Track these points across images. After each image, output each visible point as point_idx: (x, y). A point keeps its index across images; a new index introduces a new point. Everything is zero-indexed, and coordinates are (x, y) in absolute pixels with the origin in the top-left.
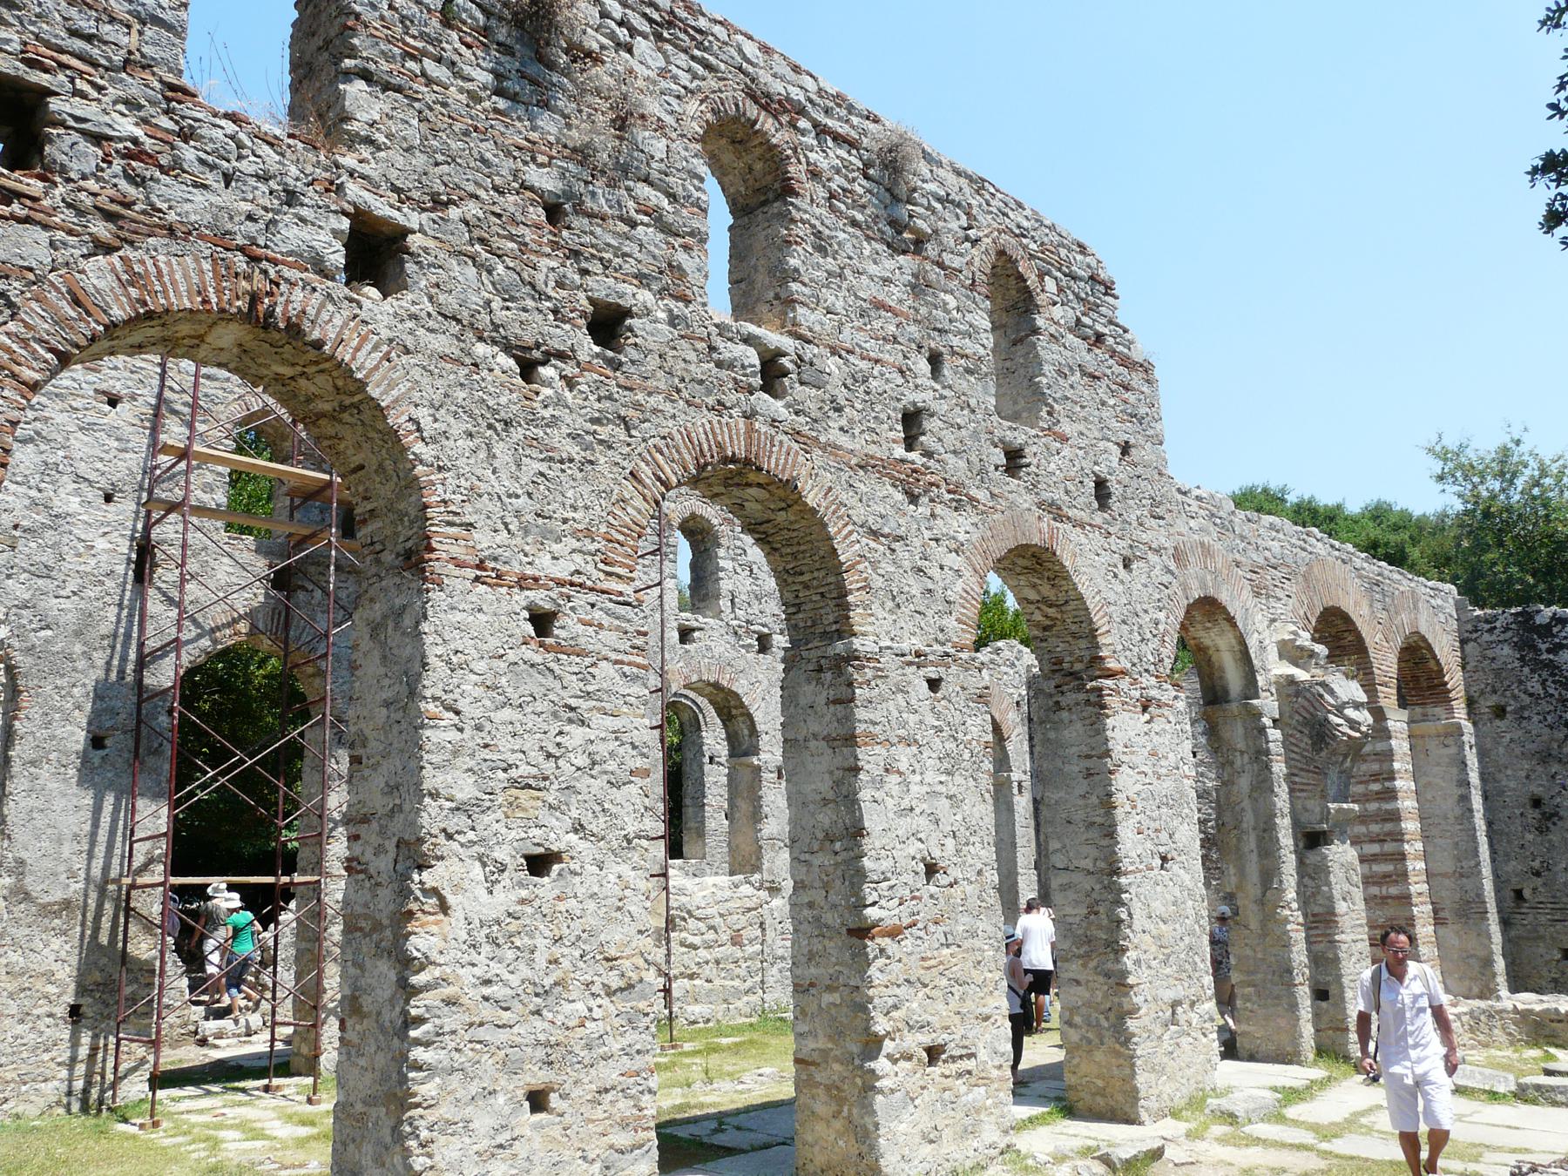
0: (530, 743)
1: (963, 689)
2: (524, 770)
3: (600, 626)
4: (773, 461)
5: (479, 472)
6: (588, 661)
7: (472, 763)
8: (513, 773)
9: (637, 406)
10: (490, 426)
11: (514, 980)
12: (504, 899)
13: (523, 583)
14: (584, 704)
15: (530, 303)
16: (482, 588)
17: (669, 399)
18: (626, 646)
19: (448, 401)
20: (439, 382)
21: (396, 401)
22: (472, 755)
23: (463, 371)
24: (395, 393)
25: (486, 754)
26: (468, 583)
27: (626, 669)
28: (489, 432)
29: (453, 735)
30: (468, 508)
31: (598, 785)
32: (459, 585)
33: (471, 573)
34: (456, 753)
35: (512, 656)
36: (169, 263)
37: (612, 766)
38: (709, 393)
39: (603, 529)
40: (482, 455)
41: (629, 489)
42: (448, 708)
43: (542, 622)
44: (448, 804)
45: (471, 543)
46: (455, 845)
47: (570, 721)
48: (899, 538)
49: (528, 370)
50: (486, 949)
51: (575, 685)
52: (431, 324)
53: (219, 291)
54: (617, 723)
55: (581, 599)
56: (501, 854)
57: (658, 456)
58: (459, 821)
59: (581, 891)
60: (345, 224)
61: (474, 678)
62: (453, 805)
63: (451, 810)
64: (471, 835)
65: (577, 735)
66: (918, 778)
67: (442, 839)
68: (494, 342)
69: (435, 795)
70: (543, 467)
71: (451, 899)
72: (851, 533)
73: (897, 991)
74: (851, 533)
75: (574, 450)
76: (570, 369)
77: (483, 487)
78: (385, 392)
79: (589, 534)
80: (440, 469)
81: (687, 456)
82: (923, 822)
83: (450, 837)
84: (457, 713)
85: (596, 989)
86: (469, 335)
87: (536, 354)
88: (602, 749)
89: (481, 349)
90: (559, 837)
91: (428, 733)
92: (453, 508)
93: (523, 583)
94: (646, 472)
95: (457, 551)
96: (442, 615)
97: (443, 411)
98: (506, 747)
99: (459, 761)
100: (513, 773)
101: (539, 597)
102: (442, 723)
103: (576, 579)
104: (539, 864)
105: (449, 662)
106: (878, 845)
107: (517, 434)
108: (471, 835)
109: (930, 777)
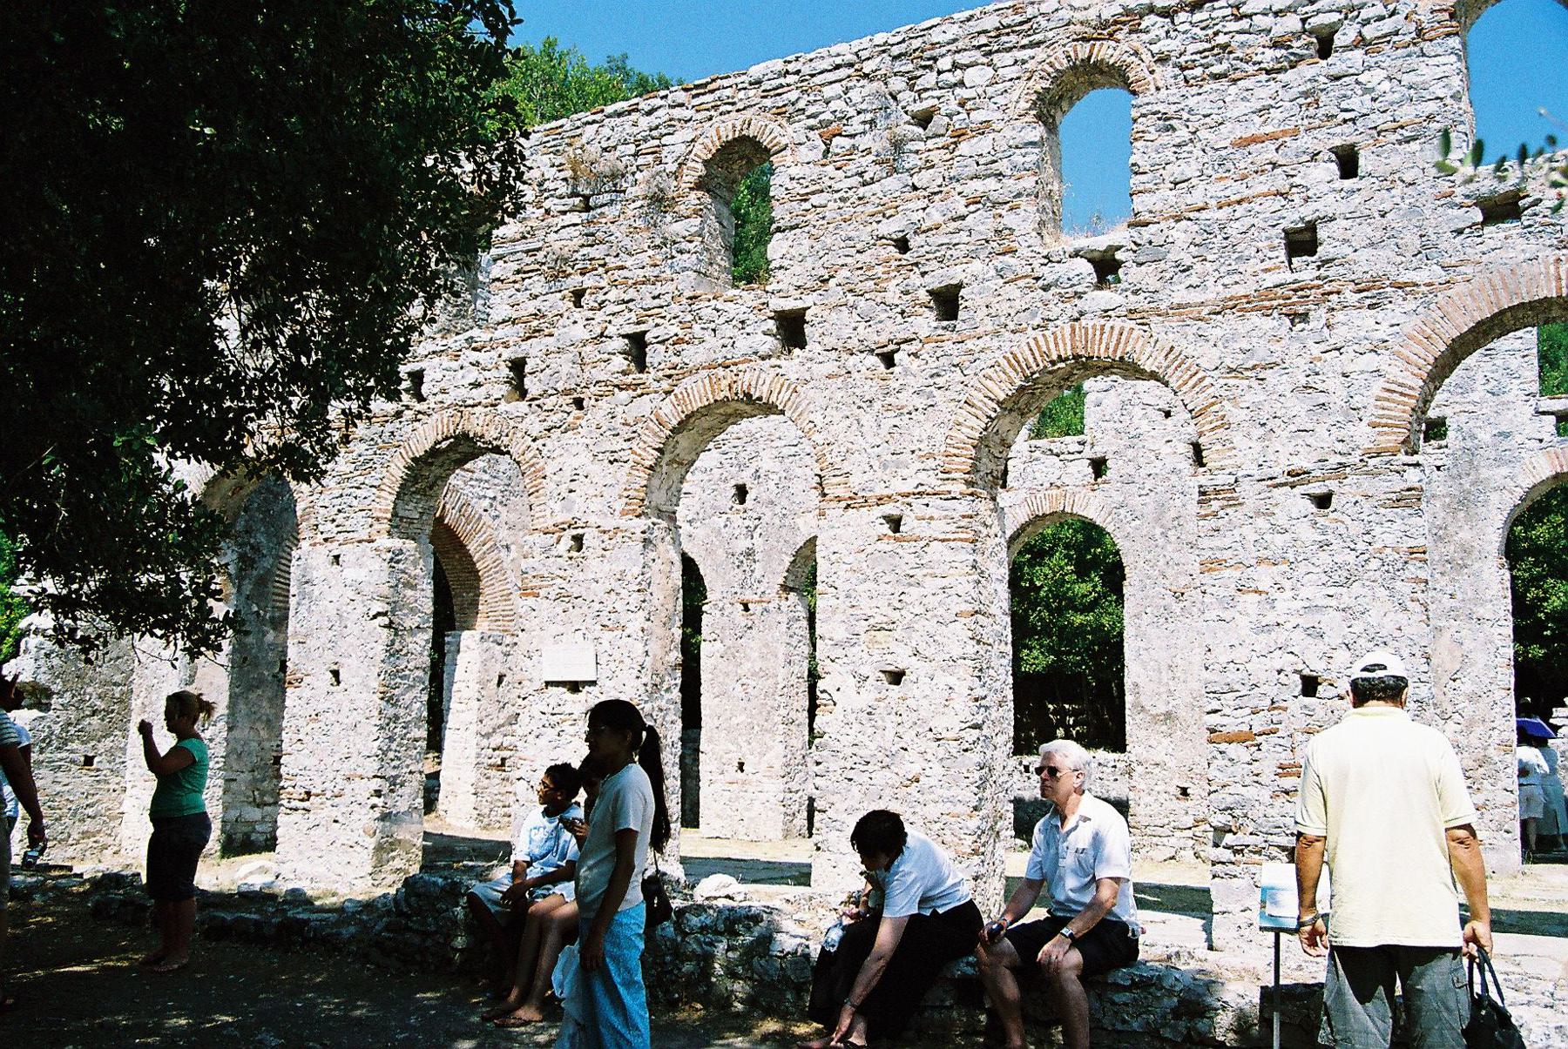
0: (882, 602)
1: (1367, 497)
2: (879, 619)
3: (931, 518)
4: (1103, 347)
6: (923, 543)
8: (872, 621)
9: (970, 352)
11: (873, 746)
12: (868, 697)
13: (880, 500)
14: (919, 573)
15: (883, 316)
17: (997, 334)
18: (953, 528)
25: (851, 611)
27: (952, 544)
29: (833, 602)
31: (931, 626)
33: (843, 504)
34: (834, 612)
35: (869, 550)
37: (941, 611)
38: (1034, 315)
39: (943, 449)
41: (962, 415)
43: (895, 523)
47: (910, 585)
48: (1272, 365)
49: (888, 360)
50: (856, 726)
51: (912, 560)
52: (821, 359)
53: (713, 392)
54: (945, 582)
55: (917, 504)
56: (864, 671)
57: (988, 383)
58: (838, 652)
59: (917, 693)
60: (771, 325)
65: (915, 592)
66: (1288, 594)
70: (897, 421)
72: (1202, 380)
73: (1243, 790)
74: (1202, 380)
75: (920, 402)
76: (913, 347)
77: (854, 447)
79: (930, 456)
81: (1013, 374)
82: (1298, 635)
85: (928, 756)
86: (844, 356)
87: (892, 347)
88: (932, 601)
89: (852, 361)
90: (901, 661)
93: (880, 500)
94: (977, 398)
98: (866, 607)
100: (872, 621)
101: (890, 509)
103: (921, 489)
104: (896, 677)
106: (1223, 659)
107: (877, 405)
109: (1304, 592)
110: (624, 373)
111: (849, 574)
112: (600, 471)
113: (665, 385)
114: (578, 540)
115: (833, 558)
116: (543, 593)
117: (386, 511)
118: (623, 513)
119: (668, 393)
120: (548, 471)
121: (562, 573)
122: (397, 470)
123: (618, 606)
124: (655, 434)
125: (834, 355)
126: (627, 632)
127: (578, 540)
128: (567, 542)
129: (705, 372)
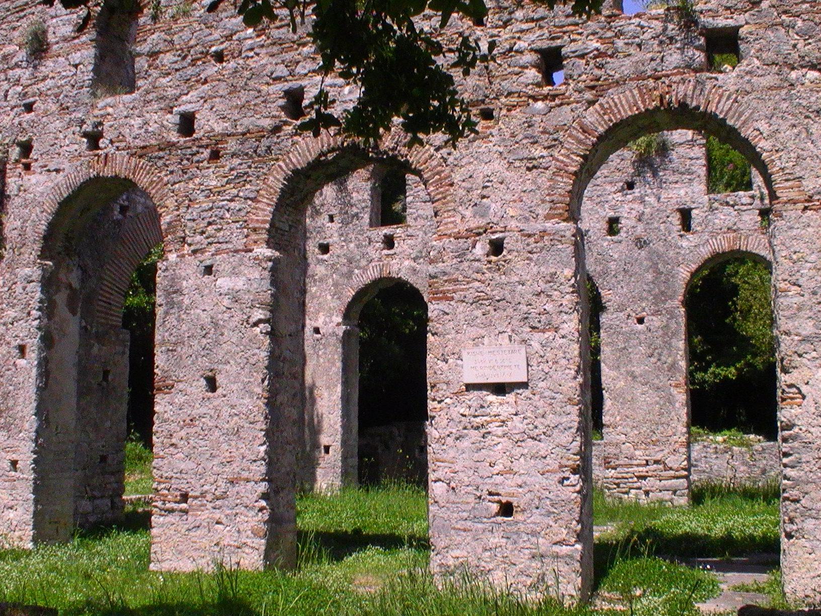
5: (802, 146)
7: (811, 314)
10: (806, 117)
16: (809, 213)
19: (777, 111)
20: (769, 104)
21: (744, 122)
22: (811, 309)
23: (784, 92)
24: (743, 118)
26: (800, 212)
28: (806, 121)
30: (798, 168)
32: (793, 214)
33: (800, 206)
34: (799, 309)
36: (619, 98)
40: (803, 135)
42: (794, 284)
44: (796, 338)
45: (802, 188)
46: (805, 361)
52: (760, 72)
53: (644, 102)
61: (808, 265)
62: (800, 338)
63: (800, 341)
64: (814, 354)
67: (796, 357)
68: (802, 67)
69: (787, 333)
71: (804, 389)
78: (737, 120)
80: (777, 151)
83: (800, 356)
84: (800, 286)
91: (781, 300)
92: (787, 171)
95: (793, 194)
96: (784, 234)
97: (774, 119)
99: (801, 314)
102: (790, 293)
105: (791, 259)
108: (814, 354)
110: (538, 85)
111: (812, 273)
112: (520, 180)
113: (588, 95)
114: (497, 247)
115: (795, 257)
116: (456, 296)
117: (264, 222)
118: (548, 217)
119: (591, 103)
120: (457, 177)
121: (479, 276)
122: (276, 181)
123: (549, 307)
124: (580, 142)
125: (775, 69)
126: (562, 332)
127: (497, 247)
128: (481, 249)
129: (634, 84)
